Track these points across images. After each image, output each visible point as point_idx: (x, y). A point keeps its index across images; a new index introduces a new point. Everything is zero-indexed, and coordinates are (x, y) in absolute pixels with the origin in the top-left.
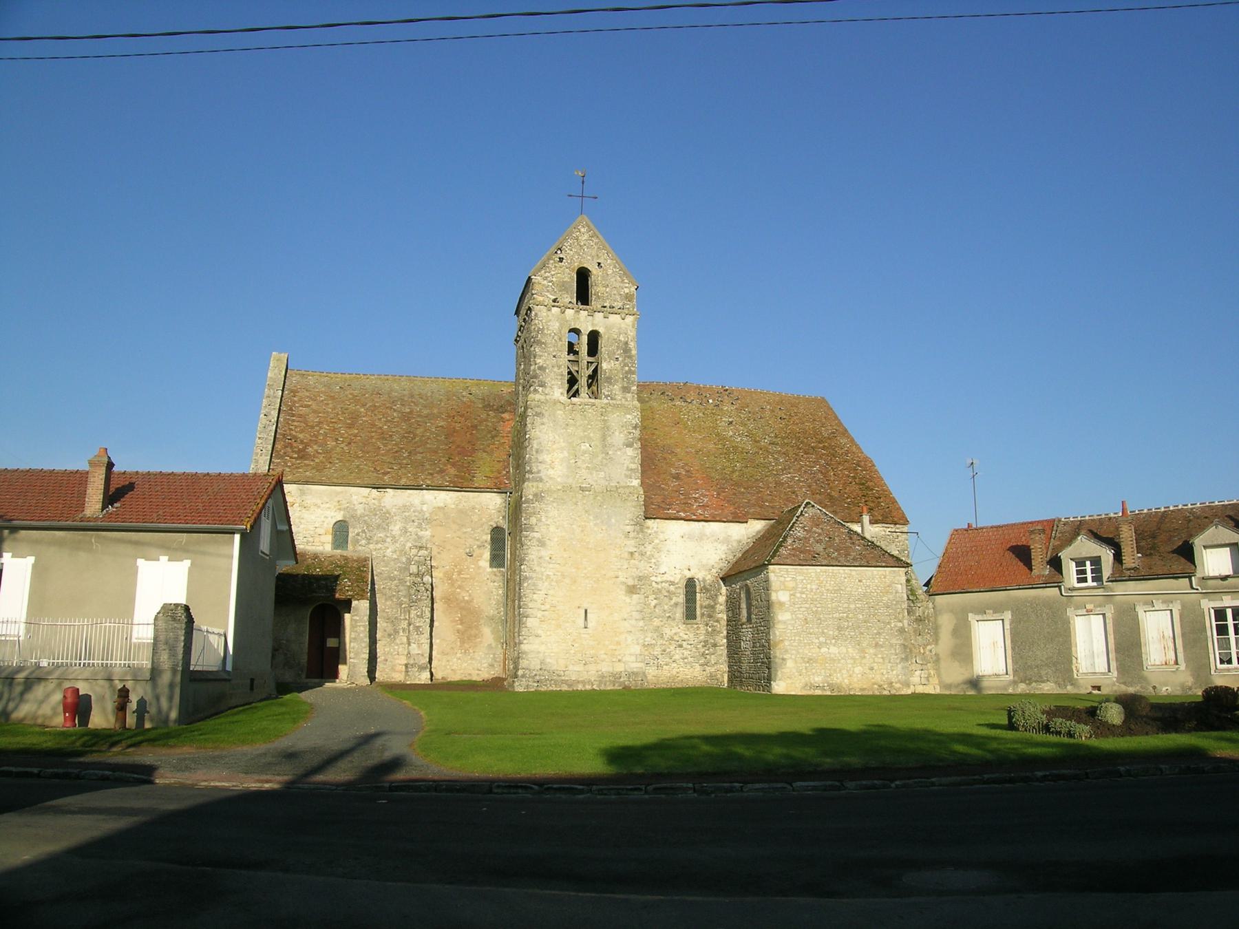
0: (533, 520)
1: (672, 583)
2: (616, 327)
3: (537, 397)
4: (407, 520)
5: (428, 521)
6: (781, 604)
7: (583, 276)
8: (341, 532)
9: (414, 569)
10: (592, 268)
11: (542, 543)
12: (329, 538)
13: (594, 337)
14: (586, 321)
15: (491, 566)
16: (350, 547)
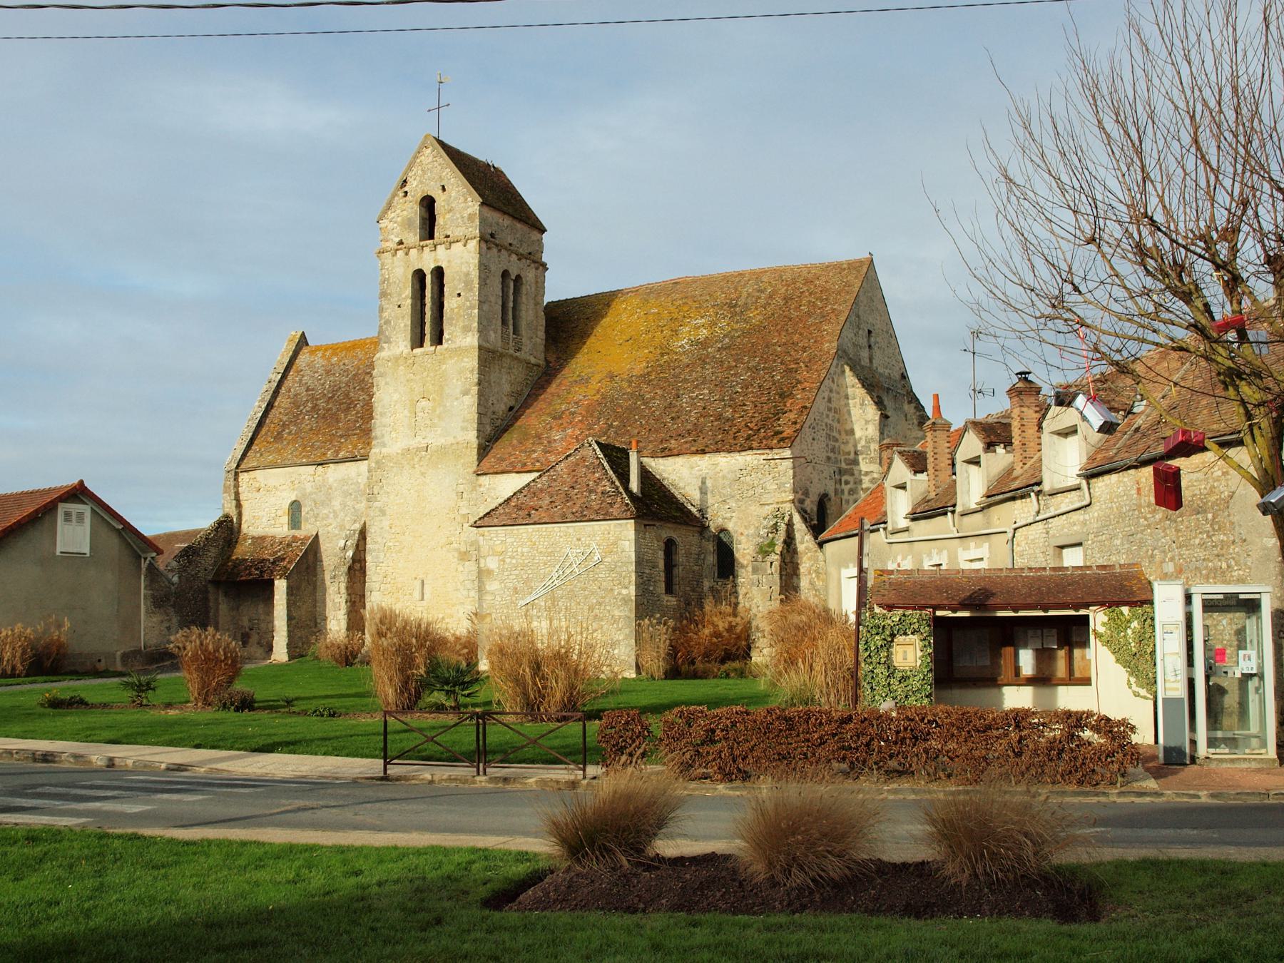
4: (347, 494)
7: (428, 204)
11: (383, 512)
12: (285, 519)
13: (439, 273)
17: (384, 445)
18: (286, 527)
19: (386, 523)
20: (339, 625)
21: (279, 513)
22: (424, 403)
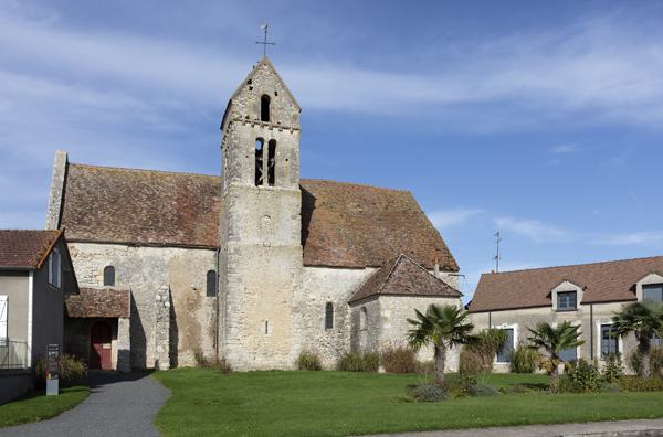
0: (234, 266)
1: (318, 306)
2: (287, 140)
3: (236, 184)
5: (168, 267)
6: (386, 318)
7: (265, 101)
8: (109, 273)
9: (158, 298)
10: (272, 95)
11: (240, 280)
12: (101, 278)
13: (273, 144)
14: (267, 135)
15: (208, 295)
16: (116, 282)
17: (239, 239)
18: (102, 284)
19: (242, 287)
20: (164, 348)
21: (95, 273)
22: (266, 219)
